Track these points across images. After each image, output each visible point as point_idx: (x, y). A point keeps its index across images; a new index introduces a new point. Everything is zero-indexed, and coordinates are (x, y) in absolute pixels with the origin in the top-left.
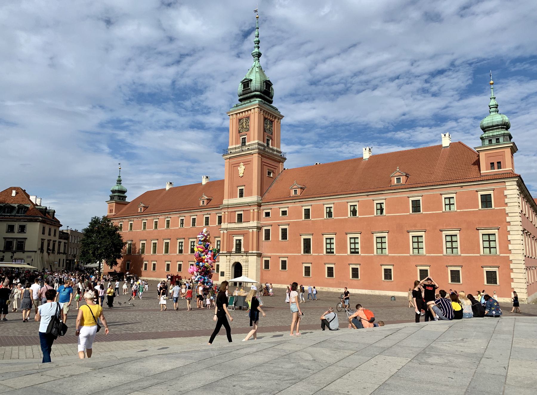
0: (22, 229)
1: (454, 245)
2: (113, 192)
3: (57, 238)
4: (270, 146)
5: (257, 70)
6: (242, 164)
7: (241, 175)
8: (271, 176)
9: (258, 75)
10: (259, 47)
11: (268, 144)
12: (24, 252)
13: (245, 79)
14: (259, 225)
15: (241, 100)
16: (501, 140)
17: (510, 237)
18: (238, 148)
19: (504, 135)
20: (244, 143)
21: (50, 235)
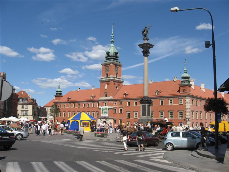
0: (27, 107)
1: (171, 116)
2: (57, 91)
3: (37, 111)
4: (118, 77)
5: (112, 48)
6: (106, 84)
7: (106, 88)
8: (118, 88)
9: (113, 50)
10: (113, 39)
11: (116, 76)
12: (27, 115)
13: (108, 52)
14: (112, 107)
15: (106, 59)
16: (186, 82)
17: (186, 113)
18: (105, 78)
19: (186, 81)
20: (107, 76)
21: (35, 109)
